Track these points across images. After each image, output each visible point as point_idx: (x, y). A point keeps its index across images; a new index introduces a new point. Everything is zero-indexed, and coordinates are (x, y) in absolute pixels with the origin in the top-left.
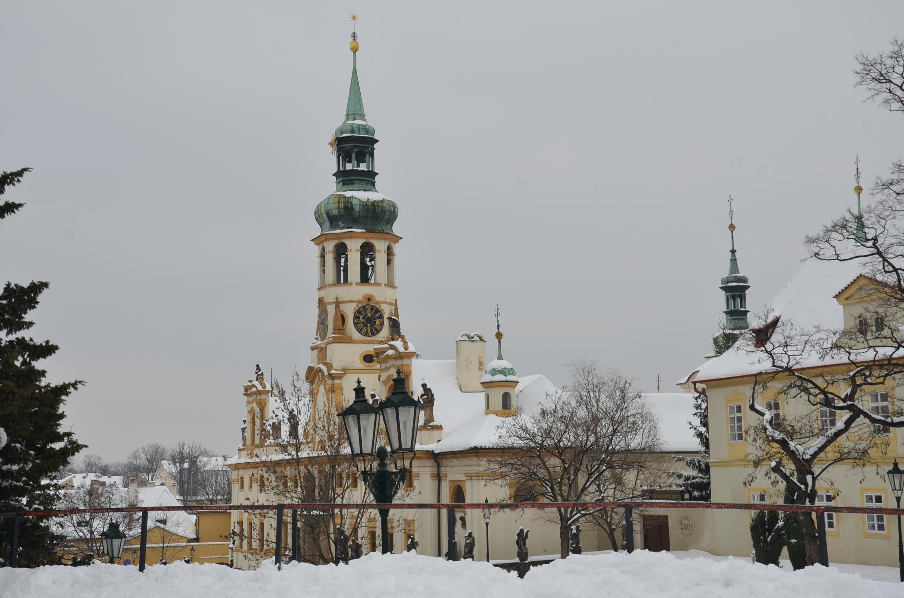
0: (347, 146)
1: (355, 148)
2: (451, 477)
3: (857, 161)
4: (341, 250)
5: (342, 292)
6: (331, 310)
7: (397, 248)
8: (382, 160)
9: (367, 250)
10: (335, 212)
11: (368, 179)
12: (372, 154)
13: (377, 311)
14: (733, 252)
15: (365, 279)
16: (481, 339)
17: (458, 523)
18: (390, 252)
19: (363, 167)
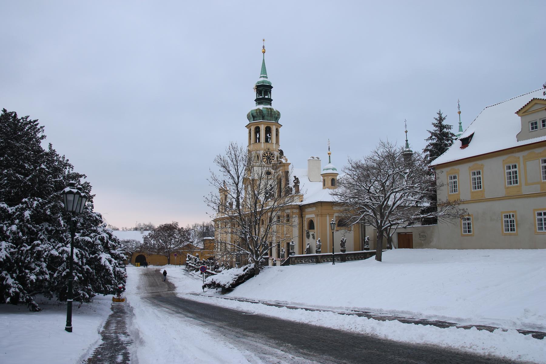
0: (261, 88)
1: (263, 91)
2: (308, 216)
3: (459, 102)
4: (257, 130)
5: (257, 146)
6: (253, 153)
7: (280, 130)
8: (274, 94)
9: (268, 130)
10: (255, 114)
11: (269, 101)
12: (270, 93)
13: (272, 154)
14: (407, 141)
15: (267, 141)
16: (318, 158)
17: (311, 237)
18: (277, 131)
19: (266, 97)
